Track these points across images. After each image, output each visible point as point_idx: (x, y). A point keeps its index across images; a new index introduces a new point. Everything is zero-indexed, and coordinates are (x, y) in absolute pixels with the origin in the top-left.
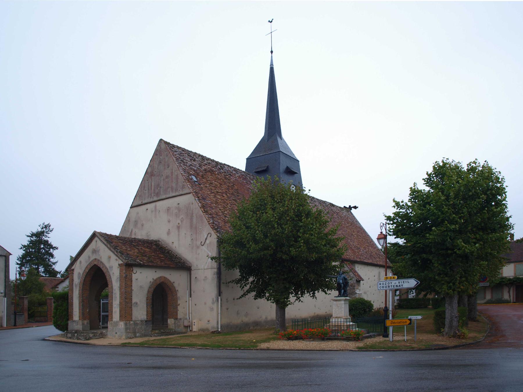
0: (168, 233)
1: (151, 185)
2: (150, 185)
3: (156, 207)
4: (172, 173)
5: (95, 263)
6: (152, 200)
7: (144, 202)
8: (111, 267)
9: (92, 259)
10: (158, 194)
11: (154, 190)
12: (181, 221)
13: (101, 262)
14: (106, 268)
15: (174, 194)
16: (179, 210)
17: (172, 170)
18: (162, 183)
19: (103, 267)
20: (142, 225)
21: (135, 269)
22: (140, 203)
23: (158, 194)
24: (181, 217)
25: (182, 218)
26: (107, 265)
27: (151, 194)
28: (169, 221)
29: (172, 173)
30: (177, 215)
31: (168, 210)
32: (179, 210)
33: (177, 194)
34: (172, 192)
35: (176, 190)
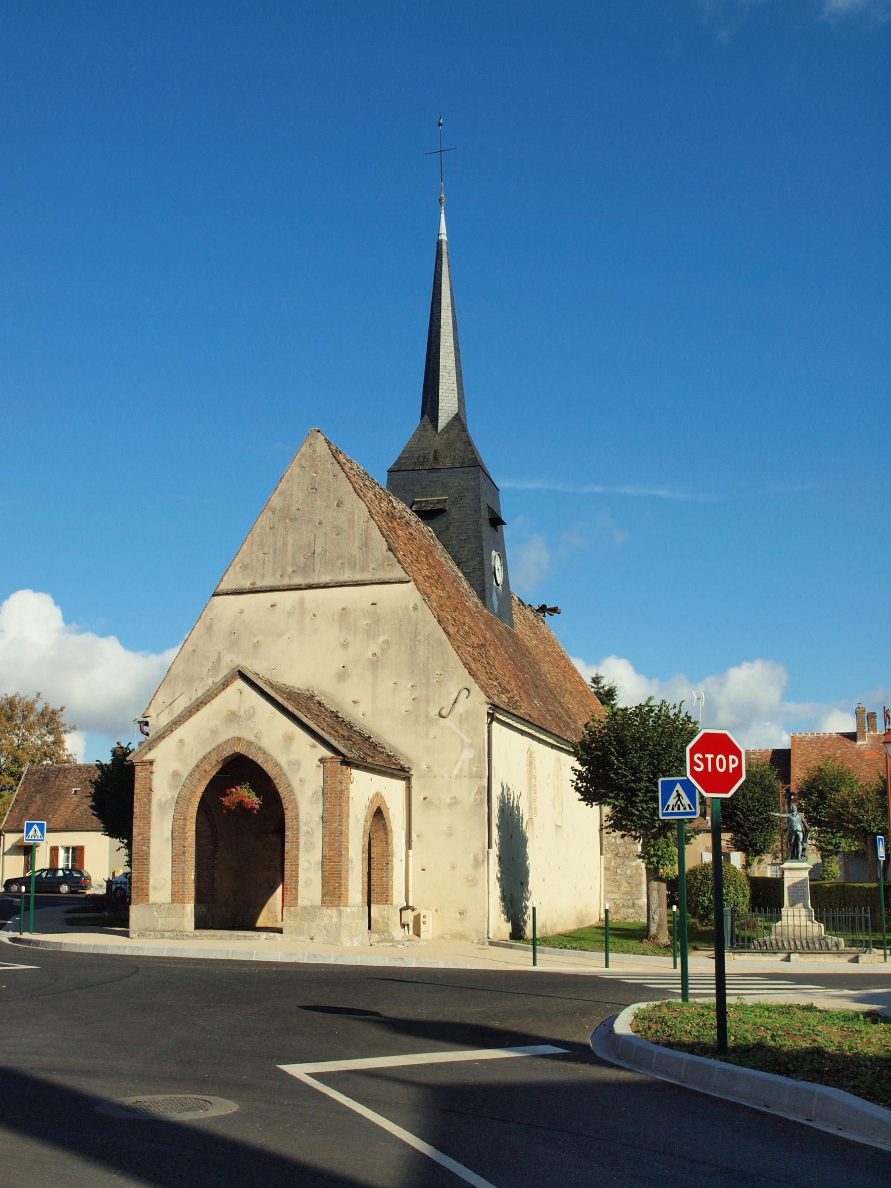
0: (343, 674)
1: (285, 543)
2: (280, 543)
3: (302, 603)
4: (351, 521)
5: (241, 749)
6: (286, 582)
7: (260, 584)
8: (296, 764)
9: (222, 738)
10: (305, 570)
11: (294, 558)
12: (382, 649)
13: (260, 749)
14: (277, 765)
15: (358, 577)
16: (376, 620)
17: (352, 513)
18: (319, 541)
19: (266, 761)
20: (257, 646)
21: (356, 774)
22: (247, 585)
23: (305, 570)
24: (382, 638)
25: (387, 642)
26: (282, 760)
27: (284, 570)
28: (345, 645)
29: (351, 521)
30: (370, 633)
31: (341, 615)
32: (376, 620)
33: (367, 577)
34: (353, 568)
35: (364, 568)
